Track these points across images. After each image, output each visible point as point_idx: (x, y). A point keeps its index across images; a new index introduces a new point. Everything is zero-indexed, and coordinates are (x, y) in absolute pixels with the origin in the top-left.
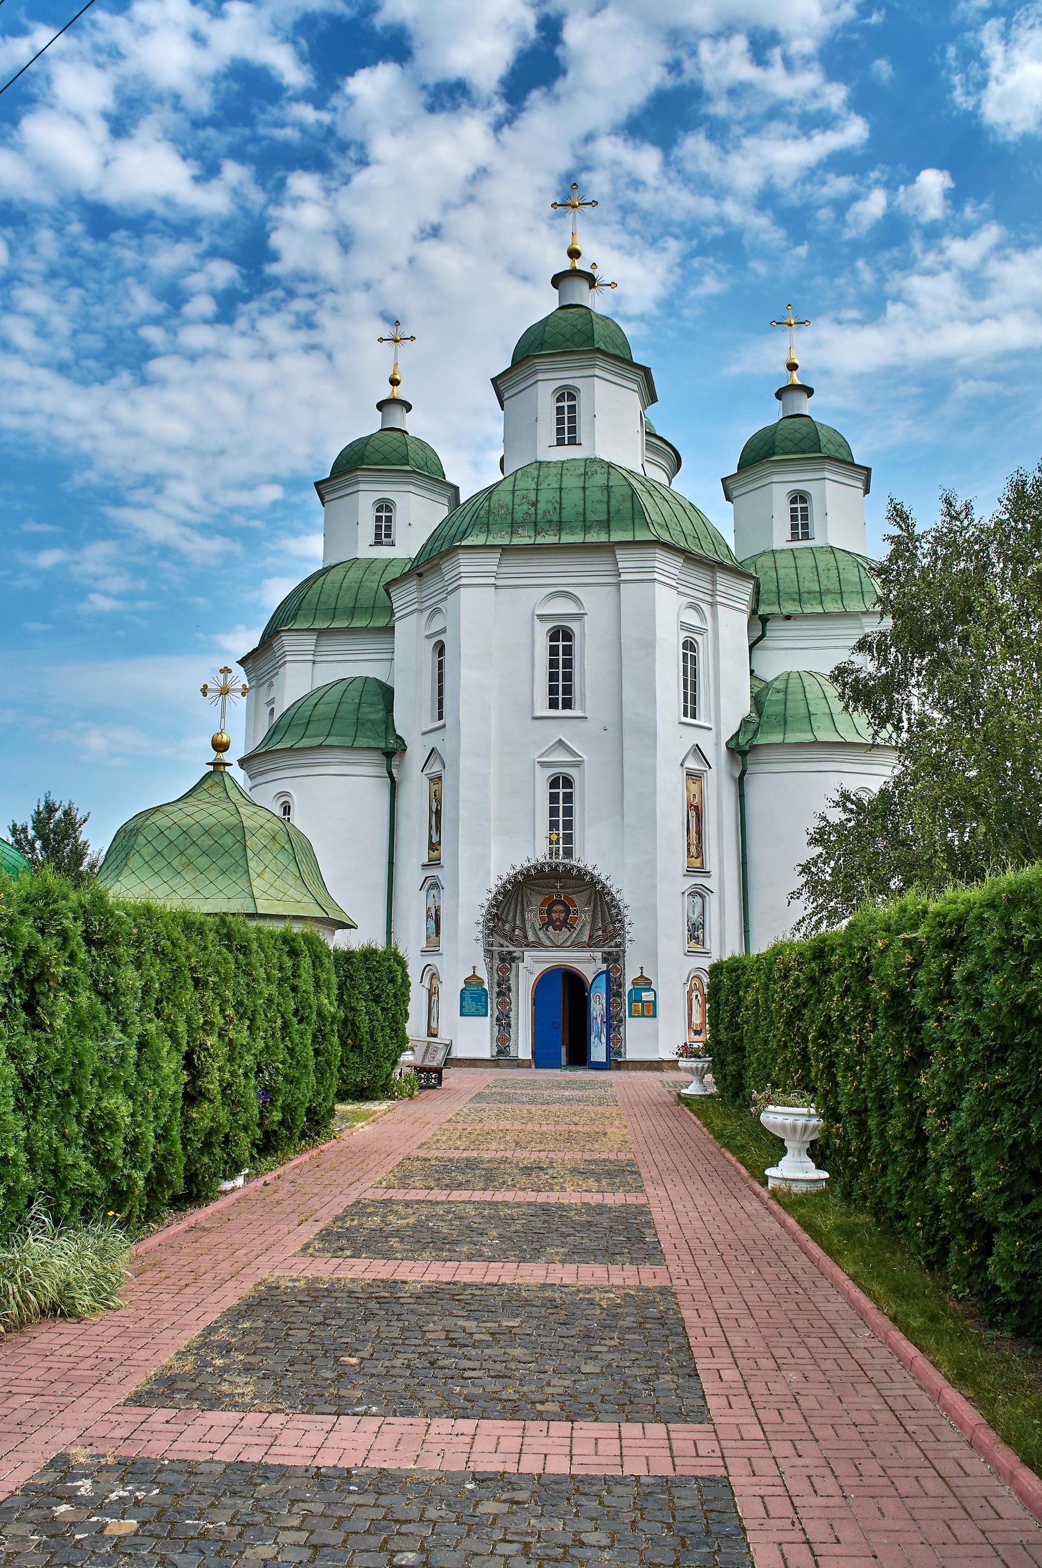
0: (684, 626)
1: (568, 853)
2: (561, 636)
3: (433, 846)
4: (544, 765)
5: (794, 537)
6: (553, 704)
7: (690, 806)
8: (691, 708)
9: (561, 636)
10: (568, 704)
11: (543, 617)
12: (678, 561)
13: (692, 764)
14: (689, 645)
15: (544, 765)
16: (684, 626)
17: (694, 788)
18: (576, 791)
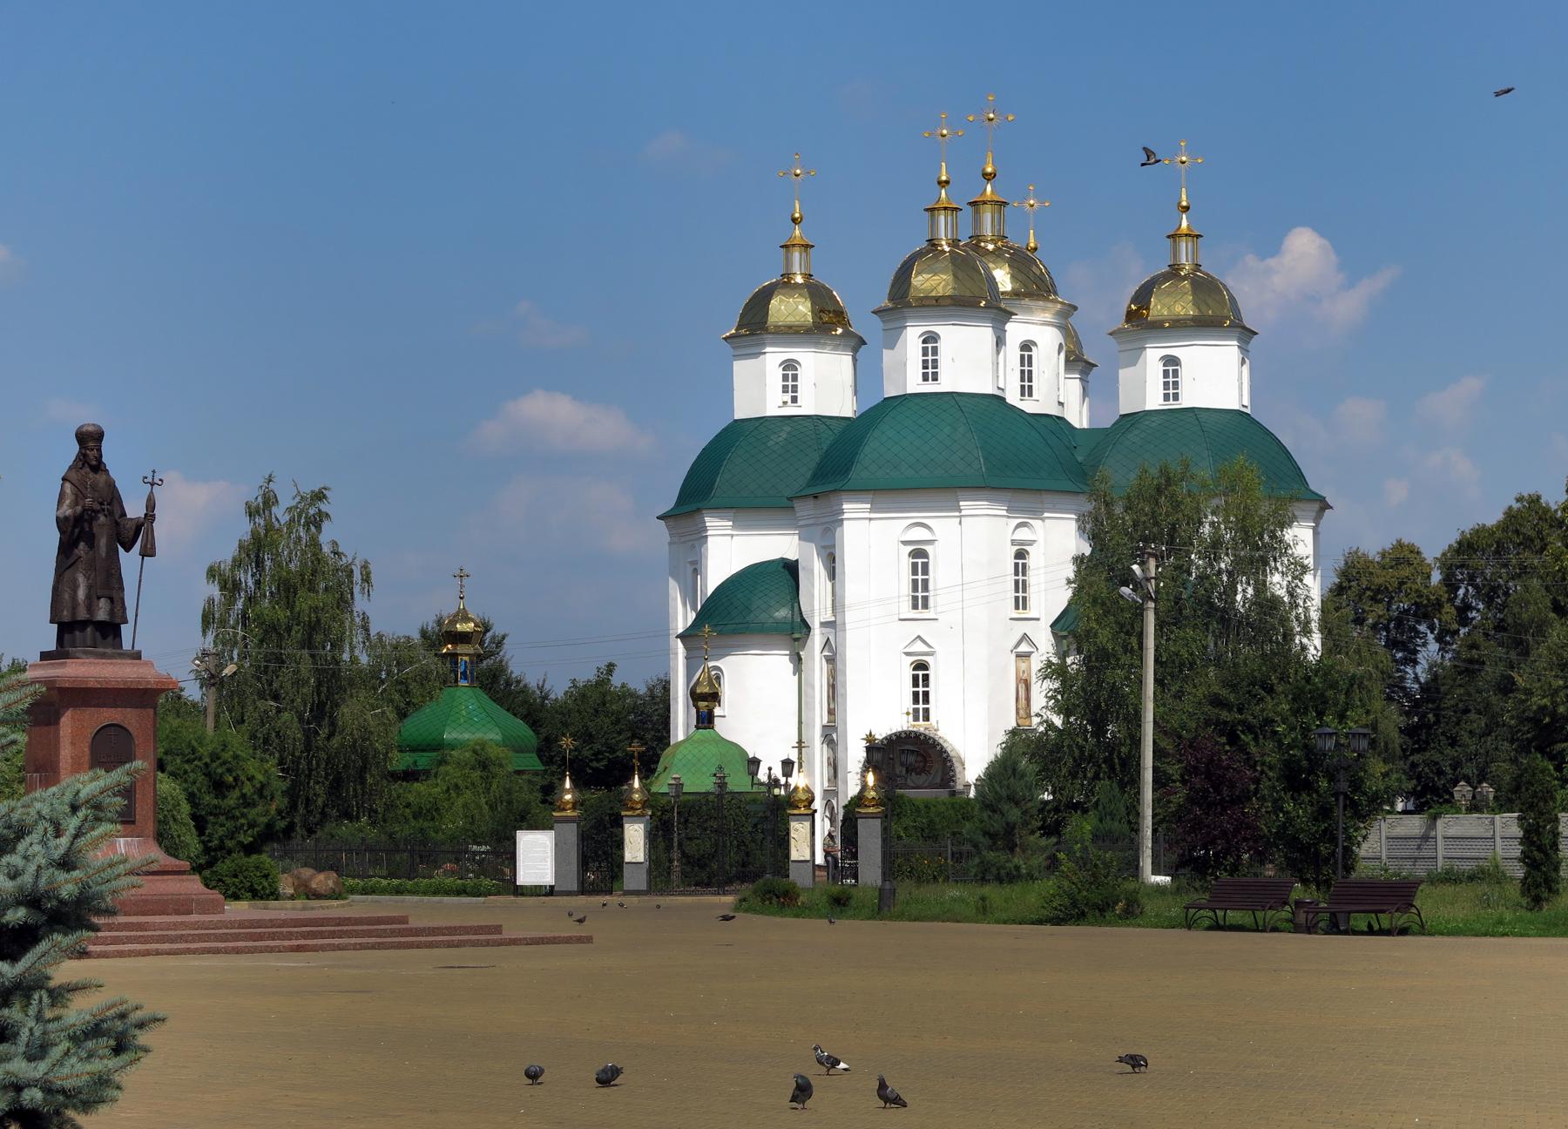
0: (1013, 542)
1: (927, 718)
2: (919, 553)
3: (831, 712)
4: (908, 654)
5: (1166, 398)
6: (915, 607)
7: (1019, 680)
8: (1021, 603)
9: (919, 553)
10: (925, 606)
11: (905, 543)
12: (1009, 495)
13: (1024, 648)
14: (1021, 555)
15: (908, 654)
16: (1013, 542)
17: (1023, 666)
18: (931, 672)
